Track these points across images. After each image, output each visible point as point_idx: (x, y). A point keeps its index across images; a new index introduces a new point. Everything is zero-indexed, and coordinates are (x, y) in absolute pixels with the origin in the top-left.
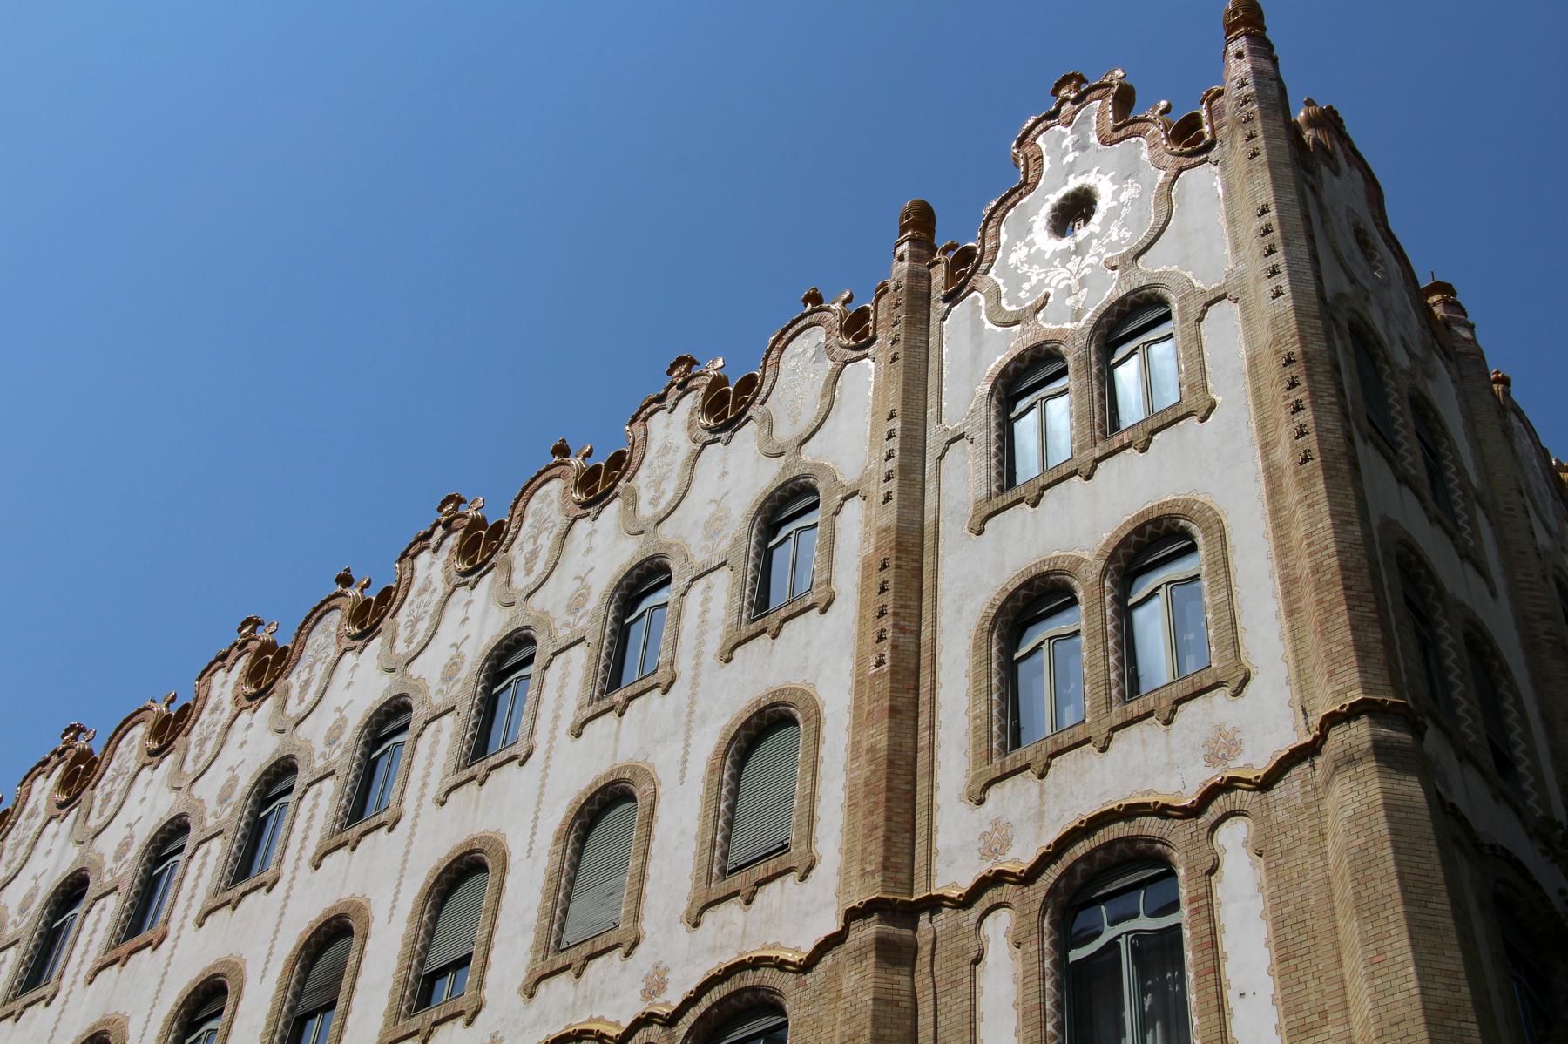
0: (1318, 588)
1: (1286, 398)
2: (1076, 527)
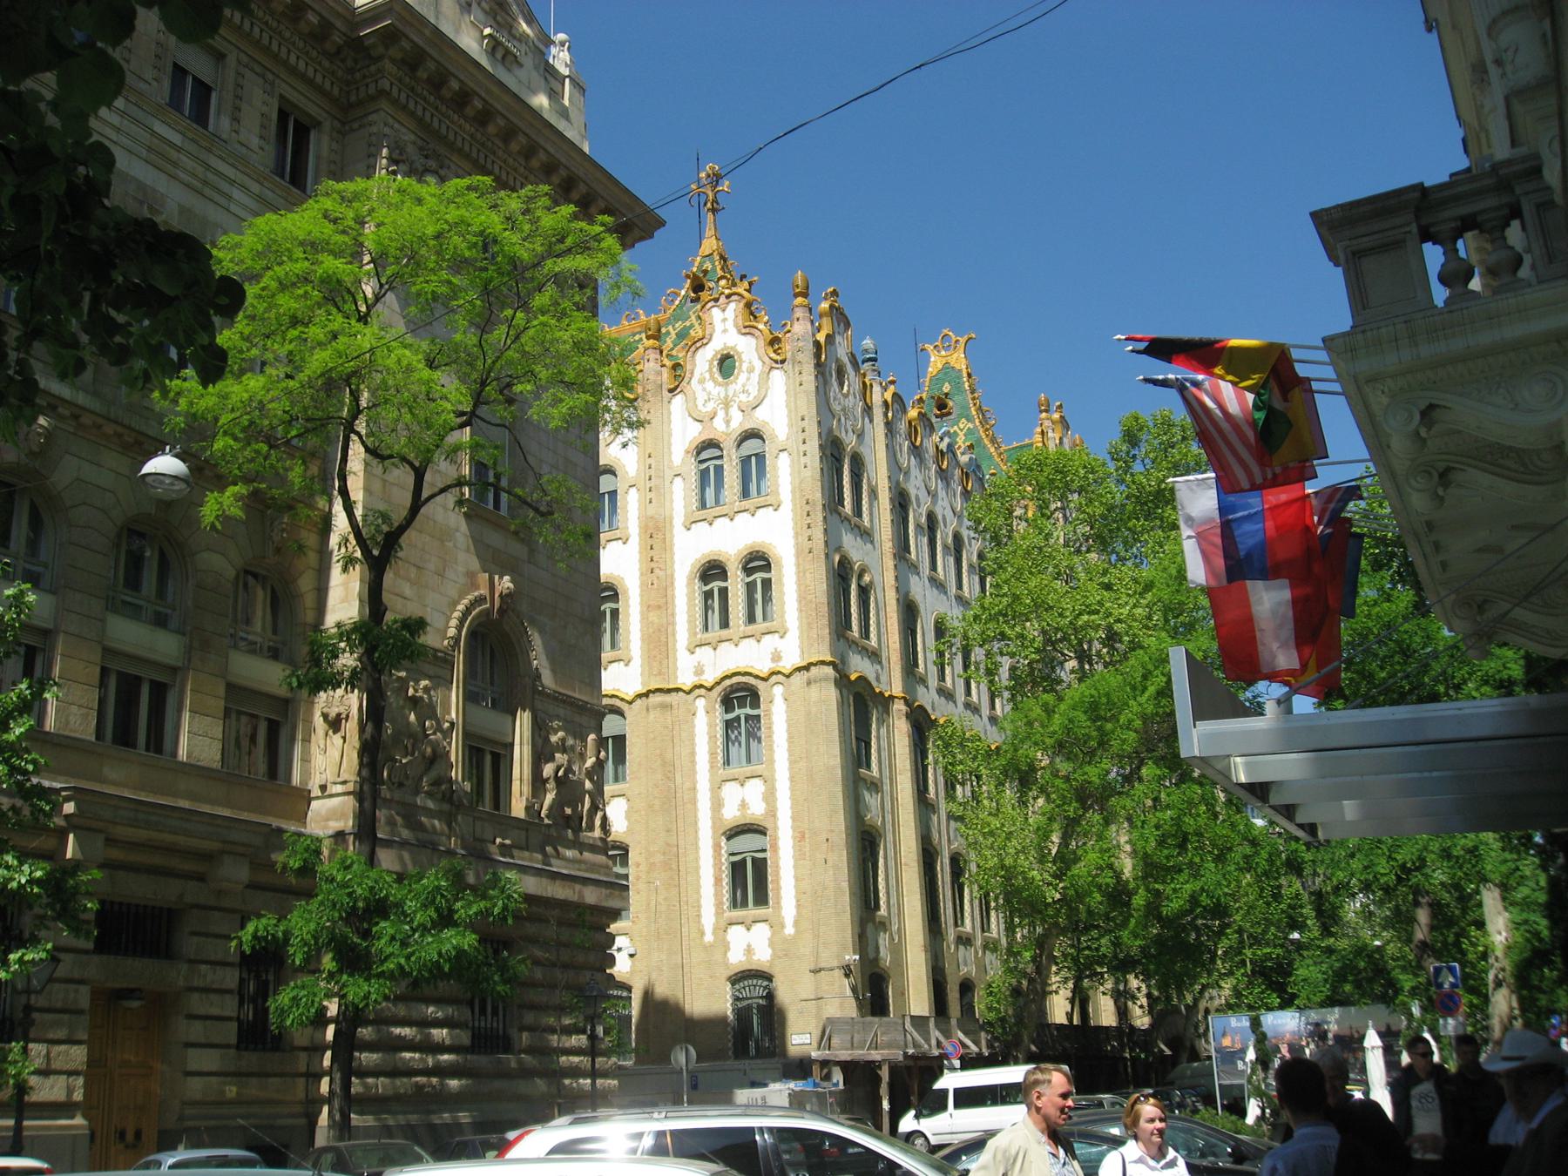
2: (729, 538)
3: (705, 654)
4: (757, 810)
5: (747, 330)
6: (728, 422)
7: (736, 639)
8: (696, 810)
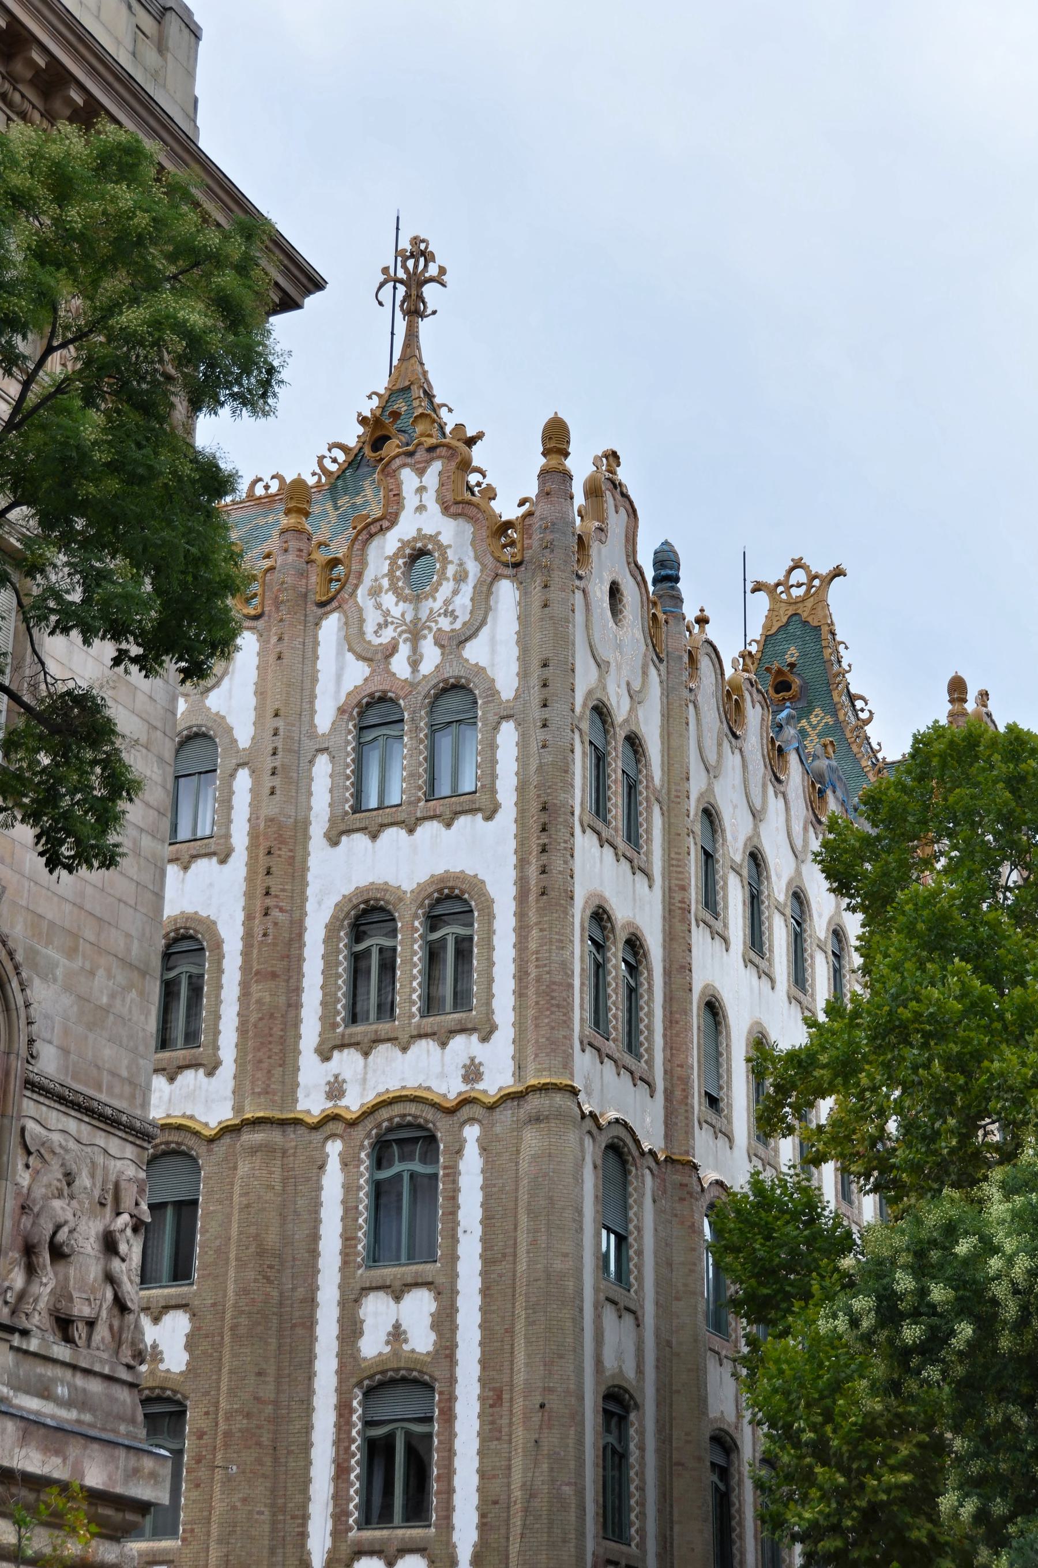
0: (538, 993)
1: (539, 838)
4: (421, 1341)
6: (415, 663)
7: (404, 1037)
8: (312, 1339)
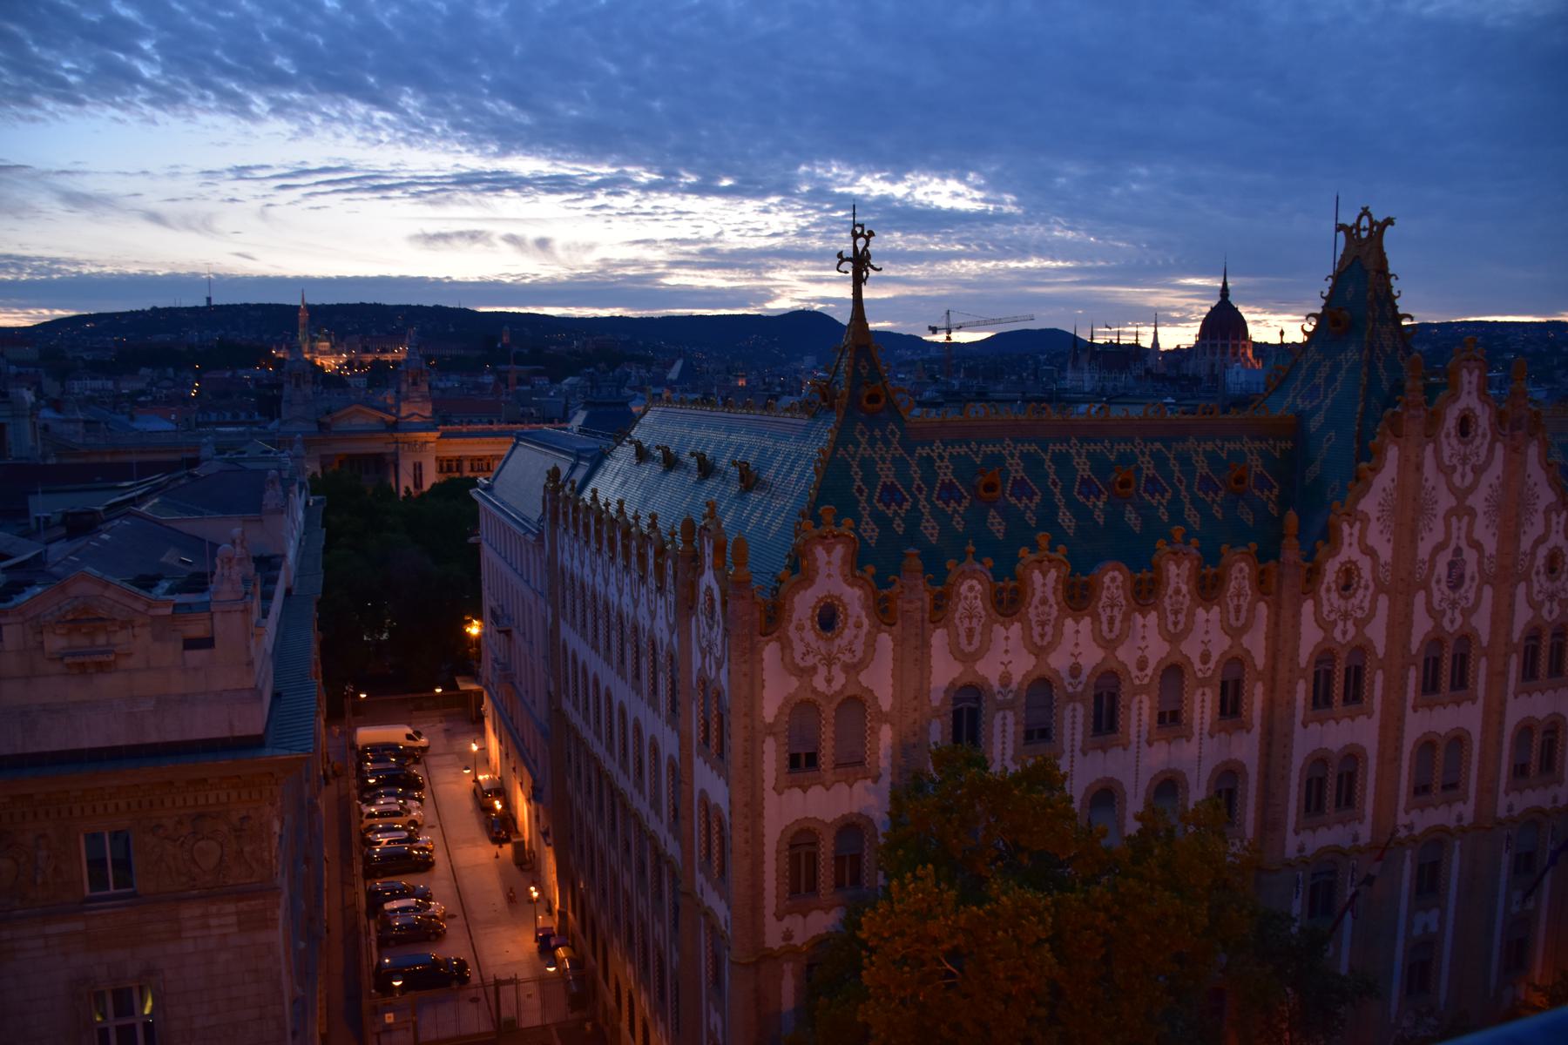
3: (794, 922)
5: (852, 580)
